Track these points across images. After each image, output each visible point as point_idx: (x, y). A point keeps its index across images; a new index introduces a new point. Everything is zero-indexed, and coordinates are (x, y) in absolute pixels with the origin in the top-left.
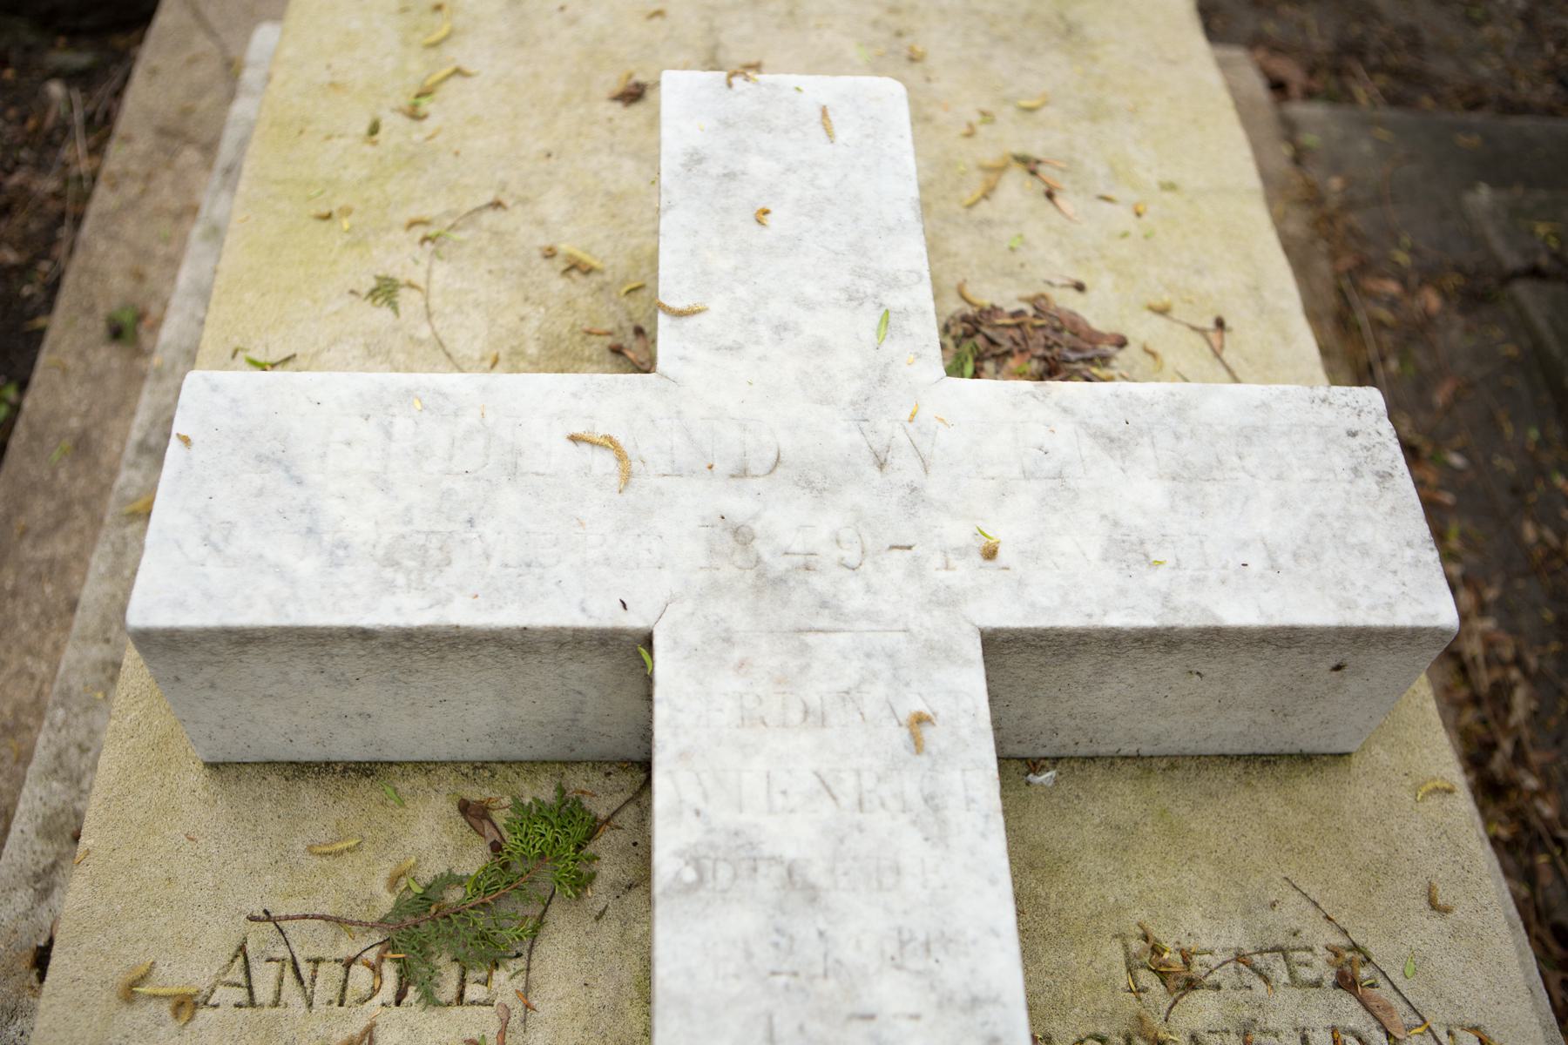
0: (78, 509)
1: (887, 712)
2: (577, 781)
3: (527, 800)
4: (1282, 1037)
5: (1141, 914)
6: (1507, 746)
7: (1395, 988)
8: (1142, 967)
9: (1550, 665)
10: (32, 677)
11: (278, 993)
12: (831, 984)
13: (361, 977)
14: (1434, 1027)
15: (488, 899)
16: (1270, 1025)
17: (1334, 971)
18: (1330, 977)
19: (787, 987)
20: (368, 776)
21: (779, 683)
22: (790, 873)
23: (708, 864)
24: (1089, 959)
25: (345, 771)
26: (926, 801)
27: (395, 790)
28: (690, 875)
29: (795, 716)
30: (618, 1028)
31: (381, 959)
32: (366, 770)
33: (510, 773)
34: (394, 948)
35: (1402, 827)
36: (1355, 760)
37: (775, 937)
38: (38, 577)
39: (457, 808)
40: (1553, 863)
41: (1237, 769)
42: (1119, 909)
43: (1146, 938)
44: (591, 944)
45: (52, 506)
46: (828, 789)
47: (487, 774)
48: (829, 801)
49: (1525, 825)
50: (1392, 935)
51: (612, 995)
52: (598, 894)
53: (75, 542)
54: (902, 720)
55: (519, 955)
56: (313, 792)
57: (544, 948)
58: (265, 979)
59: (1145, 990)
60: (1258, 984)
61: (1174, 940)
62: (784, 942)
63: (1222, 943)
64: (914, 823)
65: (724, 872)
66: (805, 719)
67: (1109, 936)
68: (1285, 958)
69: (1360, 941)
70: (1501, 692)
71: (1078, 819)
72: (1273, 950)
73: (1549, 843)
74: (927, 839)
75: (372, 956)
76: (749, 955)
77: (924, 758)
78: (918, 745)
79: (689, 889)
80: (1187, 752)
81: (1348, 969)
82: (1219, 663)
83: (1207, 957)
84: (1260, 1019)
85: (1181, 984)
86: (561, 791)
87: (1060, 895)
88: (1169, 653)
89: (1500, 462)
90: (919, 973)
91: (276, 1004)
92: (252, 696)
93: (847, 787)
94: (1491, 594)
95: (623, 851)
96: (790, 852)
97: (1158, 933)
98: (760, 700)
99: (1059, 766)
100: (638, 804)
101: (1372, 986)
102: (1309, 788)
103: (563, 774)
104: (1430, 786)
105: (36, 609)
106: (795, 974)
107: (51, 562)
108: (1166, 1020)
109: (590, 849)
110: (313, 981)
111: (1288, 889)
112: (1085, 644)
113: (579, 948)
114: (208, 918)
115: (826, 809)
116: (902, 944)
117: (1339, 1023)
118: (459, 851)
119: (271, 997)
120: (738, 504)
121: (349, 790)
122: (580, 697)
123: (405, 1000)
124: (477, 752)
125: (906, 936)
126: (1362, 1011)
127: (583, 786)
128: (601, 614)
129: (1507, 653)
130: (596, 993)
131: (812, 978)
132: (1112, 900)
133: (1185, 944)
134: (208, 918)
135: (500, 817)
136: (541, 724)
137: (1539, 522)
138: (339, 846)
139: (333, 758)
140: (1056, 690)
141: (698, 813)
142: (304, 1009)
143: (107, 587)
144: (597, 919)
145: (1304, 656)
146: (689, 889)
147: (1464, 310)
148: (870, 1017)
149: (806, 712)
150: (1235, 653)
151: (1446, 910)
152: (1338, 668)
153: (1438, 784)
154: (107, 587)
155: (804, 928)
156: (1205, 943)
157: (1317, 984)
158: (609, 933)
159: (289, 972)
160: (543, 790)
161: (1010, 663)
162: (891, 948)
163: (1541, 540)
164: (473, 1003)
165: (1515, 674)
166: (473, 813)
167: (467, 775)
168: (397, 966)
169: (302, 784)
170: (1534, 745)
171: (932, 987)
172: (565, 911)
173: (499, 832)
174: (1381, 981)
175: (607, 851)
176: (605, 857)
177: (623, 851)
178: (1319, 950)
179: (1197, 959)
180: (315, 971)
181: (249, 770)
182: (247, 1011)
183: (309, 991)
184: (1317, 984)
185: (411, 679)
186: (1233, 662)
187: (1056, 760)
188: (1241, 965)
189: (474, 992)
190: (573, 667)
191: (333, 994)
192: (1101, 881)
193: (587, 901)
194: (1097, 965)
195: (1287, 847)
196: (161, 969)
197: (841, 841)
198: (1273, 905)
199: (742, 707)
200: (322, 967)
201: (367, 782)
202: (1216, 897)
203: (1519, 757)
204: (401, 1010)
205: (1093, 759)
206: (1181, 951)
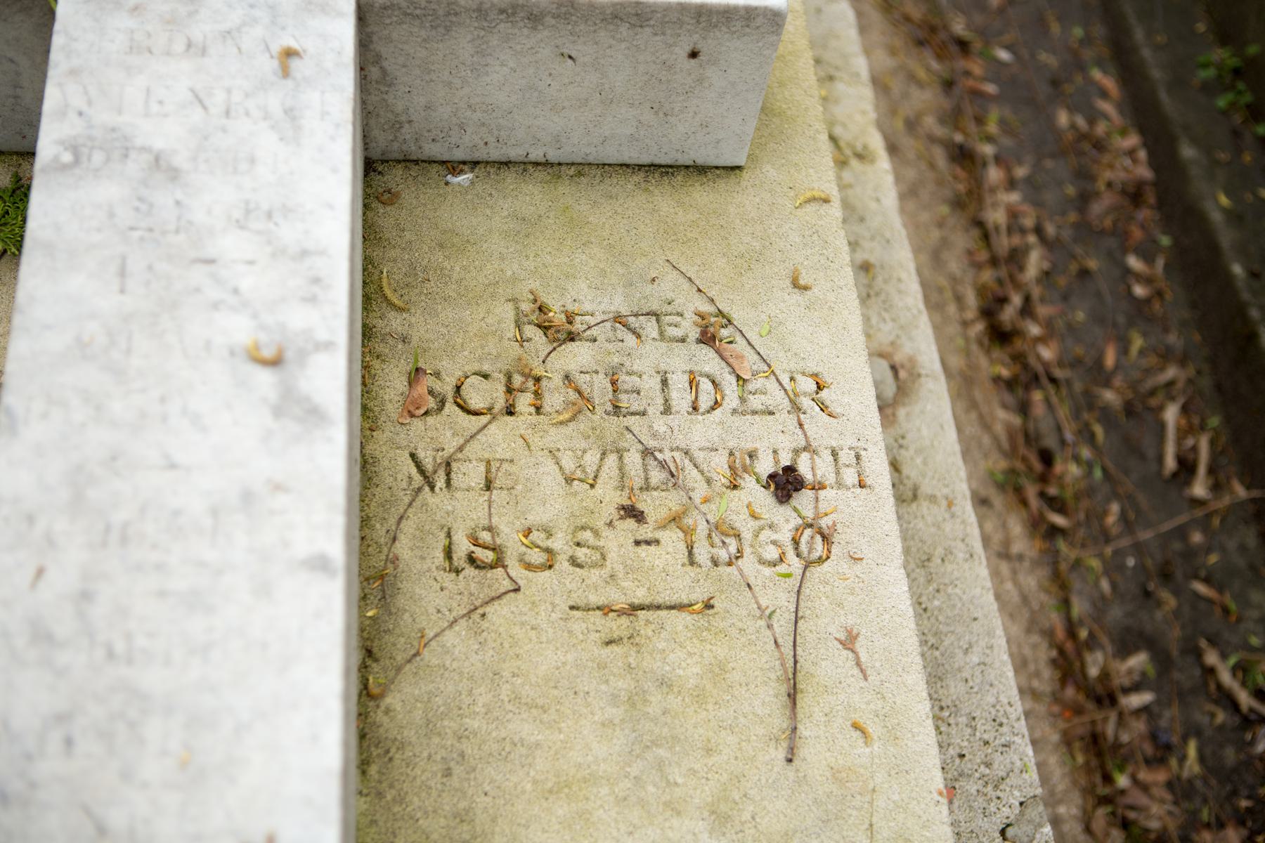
4: (644, 377)
5: (534, 284)
6: (1017, 300)
7: (750, 344)
8: (529, 323)
9: (1067, 234)
14: (778, 372)
16: (635, 368)
17: (699, 330)
18: (694, 333)
19: (142, 239)
21: (168, 22)
23: (85, 151)
24: (482, 316)
26: (286, 112)
28: (67, 157)
29: (179, 47)
35: (779, 226)
36: (745, 175)
37: (137, 204)
40: (1047, 401)
41: (639, 177)
42: (515, 280)
43: (535, 301)
46: (201, 101)
48: (199, 110)
49: (1026, 366)
50: (754, 306)
59: (529, 340)
60: (630, 340)
61: (560, 304)
62: (144, 207)
63: (602, 307)
64: (273, 127)
65: (98, 157)
67: (503, 300)
68: (658, 321)
69: (725, 309)
70: (1016, 258)
71: (488, 212)
72: (648, 314)
73: (1044, 381)
74: (281, 139)
76: (111, 215)
77: (289, 83)
78: (285, 72)
79: (64, 168)
80: (591, 159)
81: (712, 329)
82: (585, 43)
83: (587, 318)
84: (628, 364)
85: (562, 336)
87: (464, 268)
88: (534, 28)
89: (1044, 57)
90: (259, 233)
93: (217, 101)
94: (1021, 172)
96: (159, 144)
97: (545, 299)
98: (149, 35)
99: (476, 170)
101: (731, 342)
102: (702, 195)
103: (20, 165)
104: (809, 194)
106: (151, 230)
108: (544, 362)
111: (668, 268)
112: (456, 14)
115: (197, 115)
116: (248, 212)
117: (695, 368)
126: (718, 359)
129: (1029, 222)
131: (164, 233)
132: (509, 273)
133: (570, 308)
137: (1072, 109)
140: (446, 73)
141: (80, 114)
145: (658, 38)
146: (64, 168)
148: (211, 262)
149: (189, 45)
150: (595, 31)
151: (806, 288)
152: (694, 55)
153: (817, 194)
155: (164, 198)
156: (588, 307)
157: (683, 340)
161: (395, 35)
162: (237, 214)
163: (1073, 126)
165: (1032, 239)
170: (1042, 300)
171: (269, 242)
174: (739, 338)
178: (689, 315)
179: (578, 319)
184: (683, 340)
186: (596, 43)
187: (475, 164)
188: (618, 325)
192: (502, 259)
194: (489, 320)
195: (673, 238)
197: (206, 138)
198: (653, 280)
199: (132, 40)
202: (603, 273)
203: (1027, 310)
205: (507, 164)
206: (566, 312)
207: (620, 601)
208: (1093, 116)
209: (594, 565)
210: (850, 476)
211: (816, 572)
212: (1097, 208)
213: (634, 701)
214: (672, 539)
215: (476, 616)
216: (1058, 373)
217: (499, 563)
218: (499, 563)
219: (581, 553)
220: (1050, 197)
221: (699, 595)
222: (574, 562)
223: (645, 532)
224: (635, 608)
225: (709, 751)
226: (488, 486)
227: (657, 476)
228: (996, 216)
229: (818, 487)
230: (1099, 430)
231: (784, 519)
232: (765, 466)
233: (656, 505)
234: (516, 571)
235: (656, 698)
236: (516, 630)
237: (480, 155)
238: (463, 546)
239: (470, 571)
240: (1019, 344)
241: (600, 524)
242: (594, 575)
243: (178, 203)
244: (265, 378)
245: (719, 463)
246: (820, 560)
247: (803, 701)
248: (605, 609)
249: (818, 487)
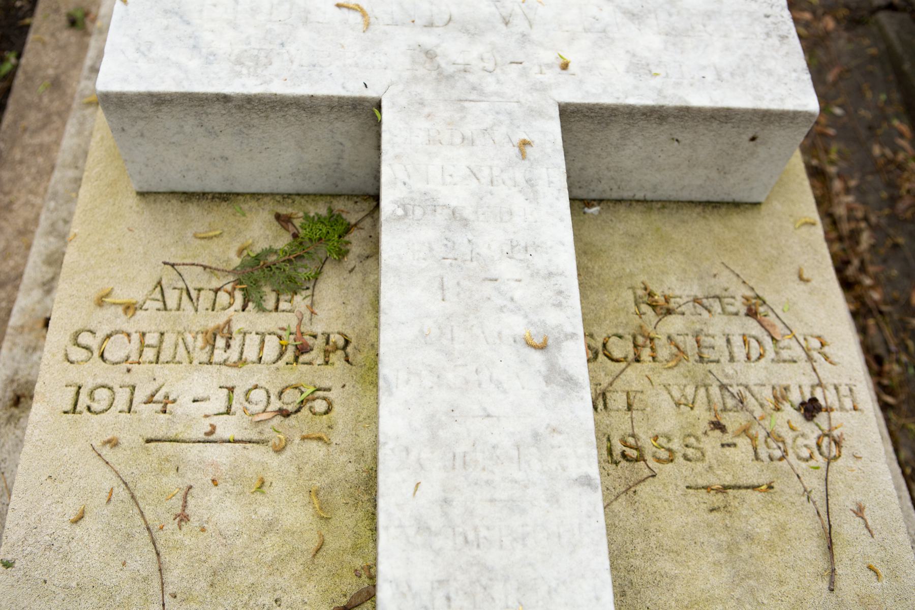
0: (55, 118)
1: (507, 139)
2: (339, 205)
3: (312, 214)
4: (716, 338)
5: (643, 278)
6: (856, 262)
7: (778, 317)
8: (643, 303)
9: (883, 222)
10: (33, 205)
11: (180, 305)
12: (475, 263)
13: (223, 298)
14: (797, 335)
15: (291, 257)
16: (710, 332)
17: (745, 308)
18: (743, 310)
19: (451, 264)
20: (226, 201)
21: (449, 124)
22: (453, 213)
24: (614, 298)
25: (213, 198)
26: (527, 181)
27: (241, 208)
28: (400, 212)
29: (458, 140)
30: (361, 324)
31: (234, 289)
32: (224, 197)
33: (303, 201)
34: (241, 283)
35: (787, 241)
36: (763, 207)
37: (445, 242)
38: (34, 153)
39: (273, 217)
40: (877, 325)
41: (699, 209)
42: (631, 275)
43: (646, 289)
44: (346, 284)
45: (40, 116)
46: (475, 175)
47: (290, 201)
48: (475, 180)
49: (864, 304)
50: (778, 292)
51: (358, 308)
52: (351, 260)
53: (54, 136)
54: (515, 144)
55: (308, 288)
56: (196, 209)
57: (321, 285)
58: (172, 298)
59: (644, 314)
60: (705, 314)
61: (661, 290)
62: (450, 244)
63: (686, 293)
64: (520, 191)
65: (418, 212)
66: (463, 142)
67: (626, 288)
68: (720, 301)
69: (761, 294)
70: (854, 236)
71: (611, 231)
72: (714, 297)
73: (875, 313)
75: (229, 287)
77: (526, 162)
78: (523, 155)
79: (400, 218)
80: (672, 198)
81: (753, 307)
82: (689, 132)
83: (678, 300)
84: (705, 329)
85: (664, 311)
86: (331, 210)
87: (601, 267)
88: (661, 124)
89: (863, 112)
91: (178, 309)
92: (164, 143)
93: (485, 173)
94: (853, 183)
95: (364, 240)
96: (454, 203)
97: (653, 287)
98: (439, 133)
99: (602, 204)
100: (372, 217)
101: (765, 316)
102: (738, 220)
103: (331, 202)
104: (803, 220)
105: (33, 170)
107: (41, 146)
108: (655, 328)
109: (346, 238)
110: (198, 299)
111: (723, 268)
112: (615, 116)
113: (340, 286)
114: (141, 268)
115: (474, 184)
116: (513, 247)
117: (747, 332)
118: (275, 238)
119: (175, 306)
120: (428, 39)
121: (215, 208)
122: (341, 147)
123: (247, 309)
124: (285, 186)
125: (515, 243)
126: (759, 327)
127: (343, 208)
128: (353, 90)
129: (860, 214)
130: (349, 307)
132: (628, 270)
133: (667, 293)
134: (141, 268)
135: (297, 222)
136: (320, 166)
137: (882, 145)
138: (211, 234)
139: (207, 190)
140: (599, 149)
142: (193, 311)
143: (75, 140)
144: (351, 271)
145: (734, 129)
146: (400, 218)
147: (847, 29)
149: (463, 139)
150: (697, 126)
151: (807, 281)
152: (753, 139)
153: (808, 220)
154: (75, 140)
155: (461, 238)
156: (677, 293)
157: (736, 314)
158: (356, 279)
159: (185, 296)
160: (321, 209)
161: (574, 128)
162: (507, 249)
163: (883, 155)
164: (283, 311)
165: (863, 225)
166: (283, 220)
167: (279, 202)
168: (243, 293)
169: (190, 205)
170: (872, 263)
171: (528, 267)
172: (332, 268)
173: (297, 229)
174: (770, 313)
176: (354, 242)
177: (364, 240)
178: (739, 298)
179: (672, 300)
180: (199, 295)
181: (161, 197)
182: (164, 313)
183: (195, 304)
184: (736, 314)
185: (250, 132)
186: (696, 132)
187: (600, 201)
188: (696, 304)
189: (283, 305)
190: (338, 124)
191: (209, 305)
192: (623, 261)
193: (344, 263)
194: (619, 301)
195: (724, 248)
196: (117, 291)
198: (715, 276)
199: (429, 135)
200: (202, 293)
201: (225, 204)
202: (684, 271)
203: (862, 269)
204: (245, 313)
205: (619, 201)
206: (665, 296)
207: (717, 484)
208: (896, 150)
209: (698, 460)
210: (848, 404)
211: (834, 465)
212: (901, 206)
213: (732, 548)
214: (743, 443)
215: (630, 493)
216: (885, 308)
217: (641, 458)
218: (641, 458)
219: (690, 452)
220: (871, 198)
221: (764, 480)
222: (686, 458)
223: (728, 438)
224: (725, 488)
225: (781, 582)
226: (630, 408)
227: (730, 403)
228: (840, 211)
229: (829, 410)
231: (811, 431)
232: (796, 397)
233: (733, 421)
234: (652, 463)
235: (744, 546)
236: (656, 502)
237: (606, 196)
238: (618, 448)
239: (624, 463)
240: (858, 290)
241: (699, 433)
242: (699, 467)
243: (469, 241)
244: (537, 357)
245: (767, 394)
246: (836, 458)
247: (836, 550)
248: (707, 488)
249: (829, 410)
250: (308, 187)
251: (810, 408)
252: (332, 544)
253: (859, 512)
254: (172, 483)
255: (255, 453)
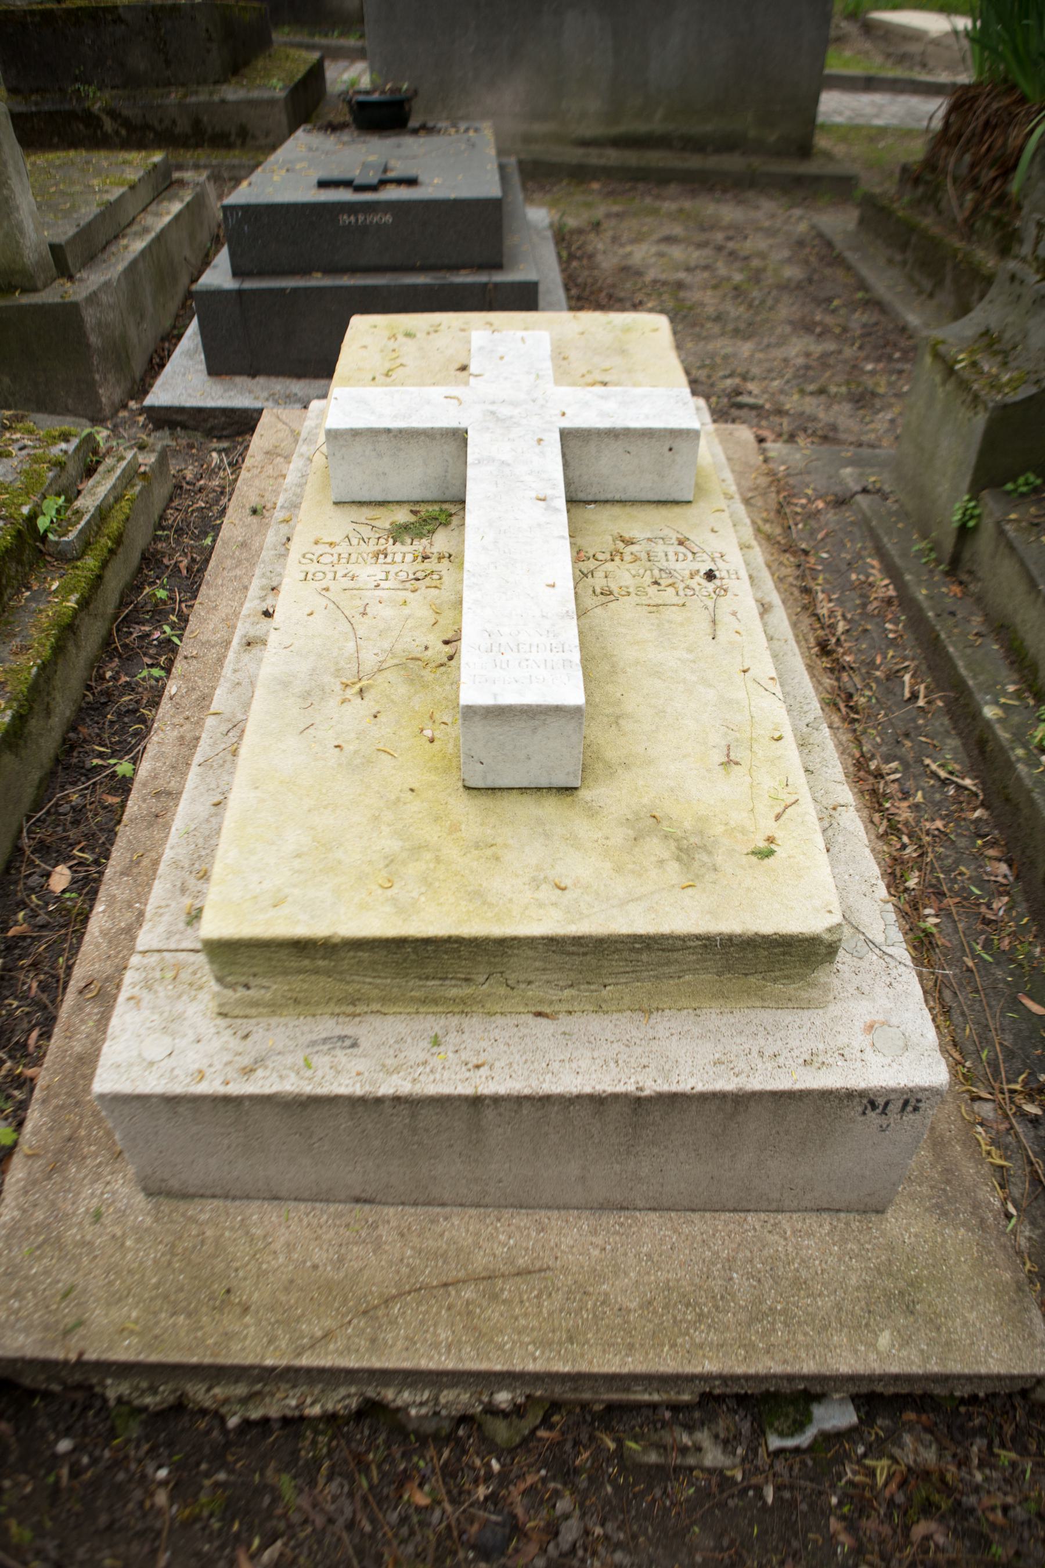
2: (445, 506)
9: (857, 618)
13: (382, 541)
40: (849, 676)
52: (452, 526)
58: (354, 541)
102: (677, 510)
120: (493, 408)
124: (416, 496)
128: (453, 424)
147: (834, 507)
158: (455, 533)
175: (455, 520)
190: (445, 447)
205: (606, 502)
207: (652, 602)
208: (868, 576)
212: (870, 608)
220: (848, 605)
221: (681, 602)
224: (658, 606)
228: (823, 611)
230: (874, 685)
231: (710, 586)
232: (702, 572)
235: (667, 626)
237: (597, 498)
238: (598, 591)
240: (835, 656)
244: (542, 503)
250: (429, 496)
251: (710, 576)
252: (441, 622)
253: (734, 614)
254: (358, 602)
255: (400, 593)
